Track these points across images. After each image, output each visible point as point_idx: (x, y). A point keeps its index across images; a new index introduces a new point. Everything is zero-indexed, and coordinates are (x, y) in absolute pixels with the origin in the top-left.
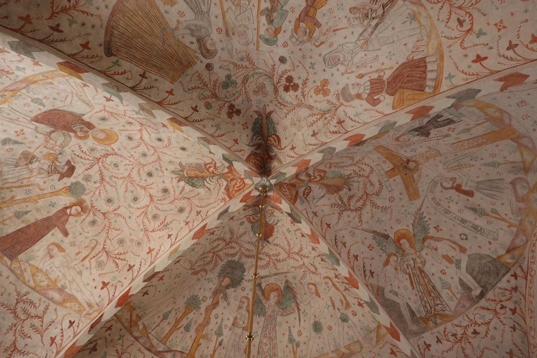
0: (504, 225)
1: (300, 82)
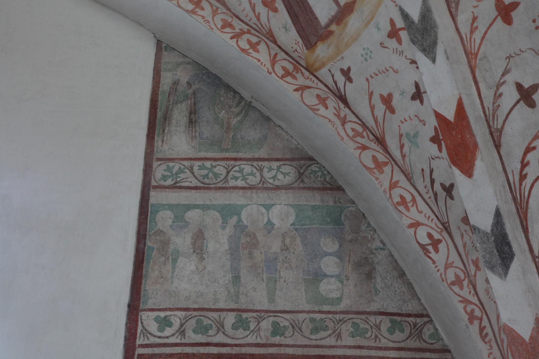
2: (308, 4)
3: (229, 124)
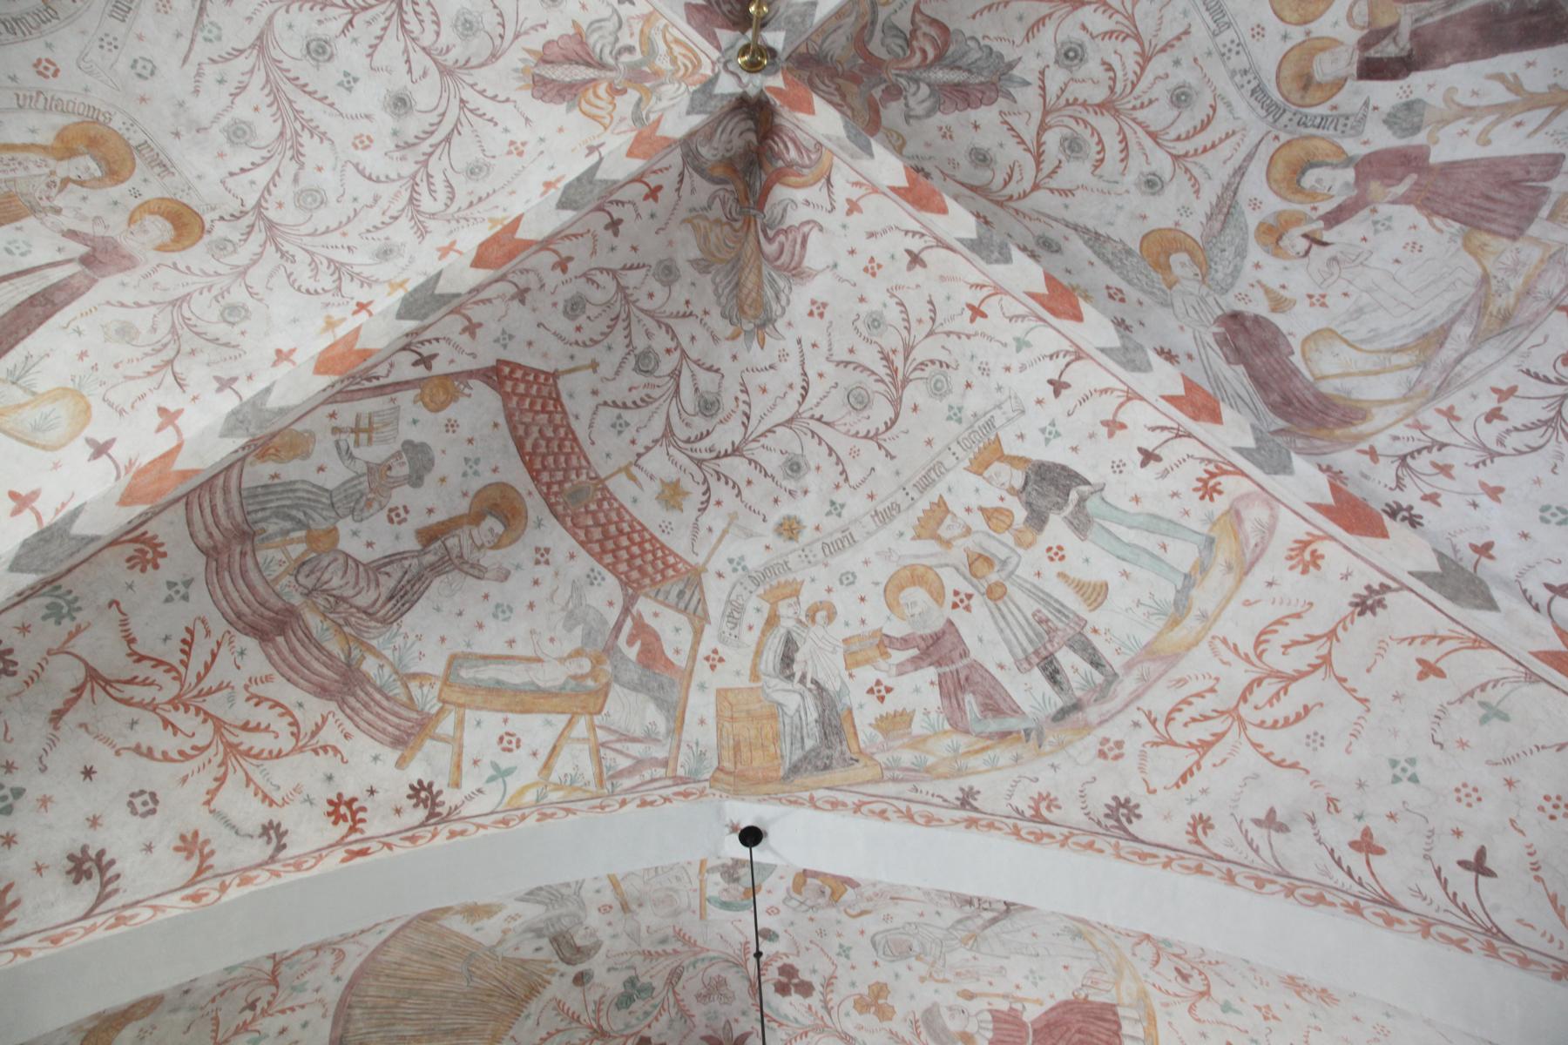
1: (816, 981)
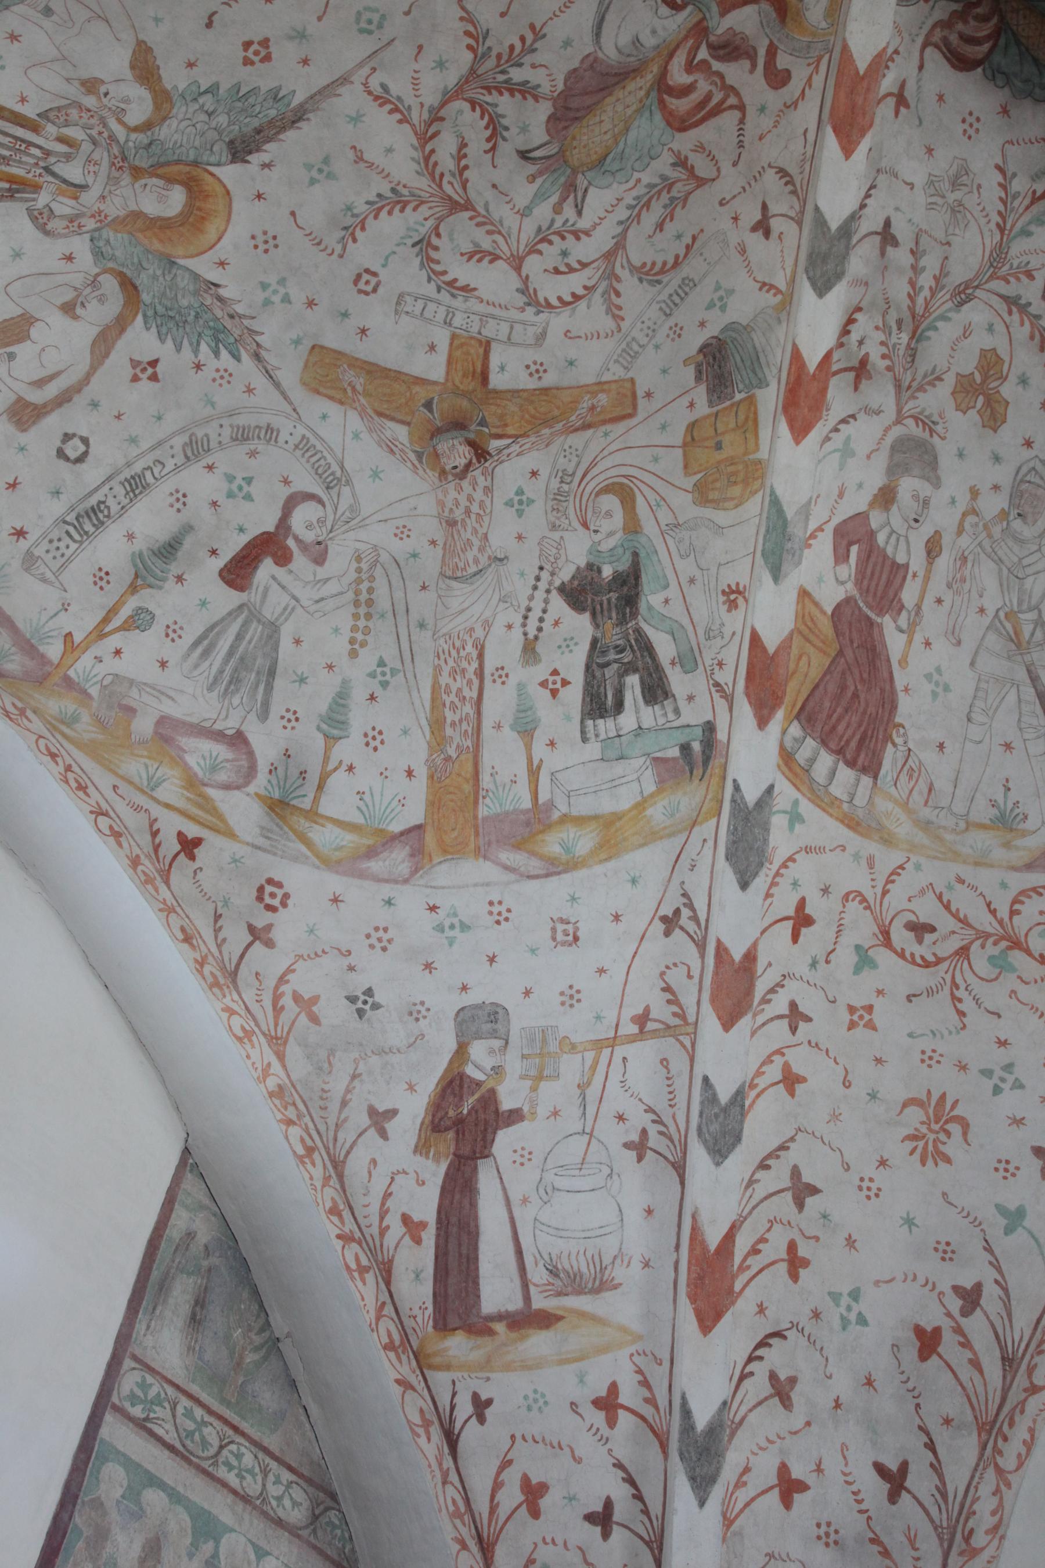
0: (81, 626)
2: (477, 1269)
3: (241, 1357)
